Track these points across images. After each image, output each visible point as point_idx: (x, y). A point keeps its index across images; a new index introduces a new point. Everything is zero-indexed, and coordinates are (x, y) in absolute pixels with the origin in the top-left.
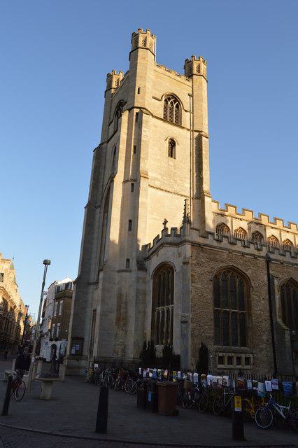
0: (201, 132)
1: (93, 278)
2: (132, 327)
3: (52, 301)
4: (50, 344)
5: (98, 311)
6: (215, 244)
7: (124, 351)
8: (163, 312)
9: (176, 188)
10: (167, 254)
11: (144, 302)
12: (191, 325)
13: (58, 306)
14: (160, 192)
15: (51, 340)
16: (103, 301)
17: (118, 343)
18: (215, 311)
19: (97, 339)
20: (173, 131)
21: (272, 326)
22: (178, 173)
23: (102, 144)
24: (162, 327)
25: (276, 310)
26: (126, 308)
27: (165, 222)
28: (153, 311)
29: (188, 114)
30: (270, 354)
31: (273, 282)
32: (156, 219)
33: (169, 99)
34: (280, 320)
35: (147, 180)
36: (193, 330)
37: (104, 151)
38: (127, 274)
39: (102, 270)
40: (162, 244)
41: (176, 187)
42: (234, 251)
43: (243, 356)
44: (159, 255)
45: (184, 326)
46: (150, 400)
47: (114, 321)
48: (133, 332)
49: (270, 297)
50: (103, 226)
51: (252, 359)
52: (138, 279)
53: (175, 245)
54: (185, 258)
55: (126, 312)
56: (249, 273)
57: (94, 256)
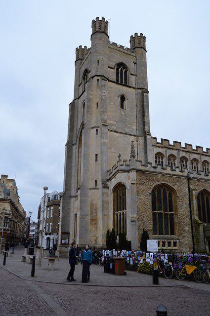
1: (73, 193)
2: (100, 224)
4: (45, 237)
5: (78, 215)
6: (152, 170)
7: (96, 240)
8: (120, 214)
9: (127, 130)
10: (121, 178)
11: (108, 209)
12: (138, 223)
13: (50, 211)
15: (46, 234)
16: (81, 208)
18: (154, 214)
20: (124, 90)
21: (191, 221)
22: (128, 119)
23: (74, 100)
24: (120, 222)
25: (194, 211)
26: (96, 212)
27: (120, 156)
28: (114, 214)
29: (133, 77)
30: (191, 239)
31: (192, 192)
32: (113, 152)
35: (106, 127)
36: (139, 225)
38: (96, 190)
39: (79, 189)
40: (118, 171)
42: (165, 174)
43: (172, 241)
45: (133, 223)
46: (111, 267)
47: (89, 221)
49: (190, 203)
50: (78, 157)
51: (178, 243)
52: (103, 194)
53: (126, 171)
56: (175, 187)
57: (73, 178)
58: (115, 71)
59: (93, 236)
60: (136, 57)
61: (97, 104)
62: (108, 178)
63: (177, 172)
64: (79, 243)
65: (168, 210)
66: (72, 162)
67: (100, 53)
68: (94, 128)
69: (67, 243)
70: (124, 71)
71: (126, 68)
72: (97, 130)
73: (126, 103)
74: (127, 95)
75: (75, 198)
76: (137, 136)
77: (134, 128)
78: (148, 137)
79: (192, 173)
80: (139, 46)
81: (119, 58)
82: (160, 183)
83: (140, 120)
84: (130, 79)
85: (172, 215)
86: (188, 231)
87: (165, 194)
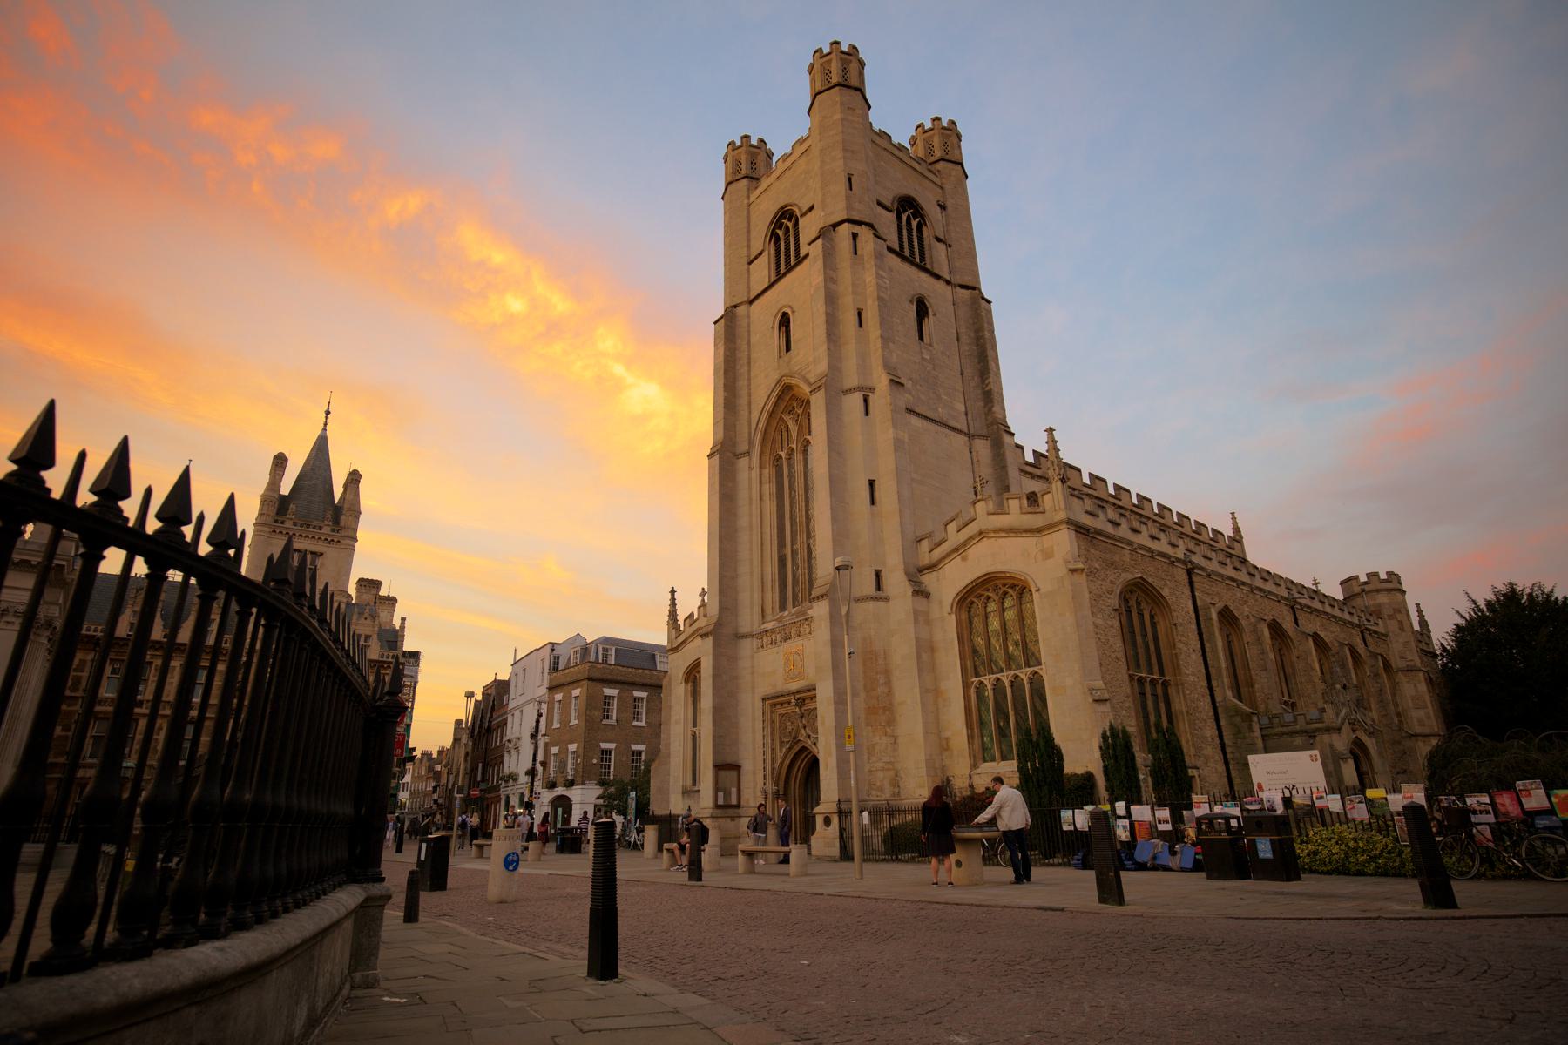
0: (974, 288)
2: (911, 722)
3: (543, 690)
5: (825, 692)
6: (1110, 529)
7: (895, 783)
9: (941, 413)
14: (915, 421)
17: (880, 765)
19: (833, 761)
20: (924, 283)
26: (888, 683)
28: (966, 686)
29: (942, 247)
30: (1221, 768)
33: (905, 211)
34: (1229, 693)
38: (881, 604)
40: (981, 534)
41: (940, 410)
50: (761, 499)
51: (1198, 779)
52: (916, 613)
56: (1165, 592)
57: (743, 569)
58: (892, 217)
59: (883, 769)
60: (942, 188)
61: (859, 314)
62: (926, 559)
63: (1162, 546)
65: (1156, 668)
67: (853, 152)
68: (855, 389)
69: (734, 802)
70: (914, 223)
71: (923, 218)
72: (866, 400)
73: (930, 323)
74: (932, 301)
76: (970, 436)
77: (956, 408)
78: (1006, 438)
79: (1195, 553)
80: (947, 157)
81: (901, 183)
82: (1130, 577)
83: (972, 384)
84: (934, 253)
85: (1165, 685)
87: (1141, 615)
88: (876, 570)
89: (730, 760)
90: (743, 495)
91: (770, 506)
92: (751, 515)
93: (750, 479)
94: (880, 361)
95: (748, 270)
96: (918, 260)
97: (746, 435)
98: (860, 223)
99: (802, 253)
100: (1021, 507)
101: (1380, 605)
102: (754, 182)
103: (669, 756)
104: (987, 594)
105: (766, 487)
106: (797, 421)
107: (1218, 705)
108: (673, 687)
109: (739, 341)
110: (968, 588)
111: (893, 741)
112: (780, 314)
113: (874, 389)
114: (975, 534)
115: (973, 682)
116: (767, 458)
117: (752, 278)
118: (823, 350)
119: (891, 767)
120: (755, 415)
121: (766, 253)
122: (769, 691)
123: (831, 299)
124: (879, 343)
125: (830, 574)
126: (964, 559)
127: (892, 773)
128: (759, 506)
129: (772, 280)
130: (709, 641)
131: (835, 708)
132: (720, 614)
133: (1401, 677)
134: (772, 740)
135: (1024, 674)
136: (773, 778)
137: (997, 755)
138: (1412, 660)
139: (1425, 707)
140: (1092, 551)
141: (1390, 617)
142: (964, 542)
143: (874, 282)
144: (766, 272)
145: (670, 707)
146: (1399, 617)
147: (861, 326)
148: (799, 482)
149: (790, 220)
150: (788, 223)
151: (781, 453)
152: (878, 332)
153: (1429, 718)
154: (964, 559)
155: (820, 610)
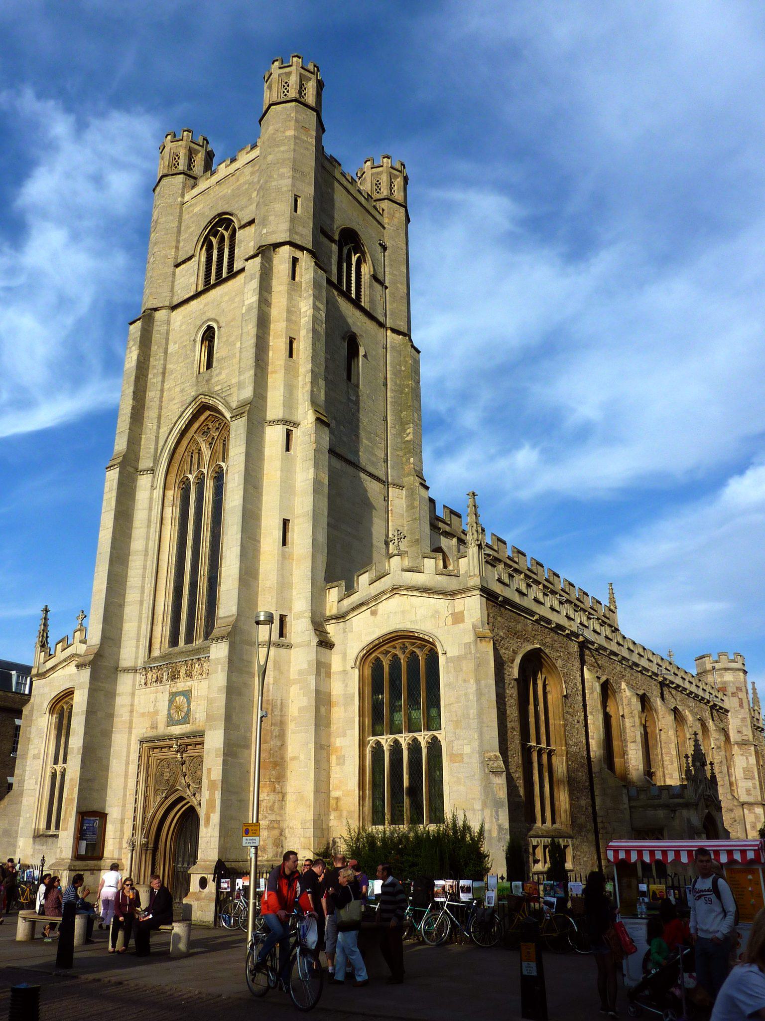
6: (517, 598)
19: (215, 818)
21: (591, 779)
26: (282, 736)
28: (362, 744)
33: (346, 244)
37: (163, 329)
38: (283, 651)
44: (380, 612)
48: (311, 796)
50: (161, 523)
53: (438, 593)
54: (474, 627)
55: (283, 746)
64: (222, 849)
65: (543, 738)
66: (130, 537)
71: (363, 253)
72: (289, 434)
75: (140, 678)
82: (529, 647)
85: (550, 754)
86: (587, 809)
88: (280, 615)
89: (95, 807)
90: (140, 515)
91: (170, 533)
92: (148, 539)
93: (151, 499)
94: (308, 396)
95: (174, 274)
96: (353, 296)
97: (152, 451)
98: (301, 248)
99: (237, 266)
100: (436, 568)
101: (725, 683)
102: (192, 181)
103: (21, 794)
104: (393, 651)
105: (168, 511)
106: (211, 444)
107: (593, 775)
108: (34, 718)
109: (154, 348)
110: (374, 644)
111: (281, 799)
112: (204, 327)
113: (298, 425)
114: (387, 590)
115: (369, 742)
116: (172, 478)
117: (176, 283)
118: (249, 375)
119: (276, 825)
120: (164, 430)
121: (195, 259)
122: (151, 733)
123: (263, 322)
124: (308, 379)
125: (233, 615)
126: (374, 613)
127: (276, 832)
128: (158, 530)
129: (199, 290)
130: (86, 673)
131: (223, 760)
132: (101, 644)
133: (736, 749)
134: (146, 787)
135: (423, 738)
136: (143, 829)
137: (387, 817)
138: (746, 735)
139: (753, 778)
140: (499, 619)
141: (734, 695)
142: (375, 596)
143: (310, 312)
144: (194, 279)
145: (29, 739)
146: (742, 695)
147: (291, 355)
148: (208, 508)
149: (226, 229)
150: (224, 232)
151: (190, 476)
152: (309, 366)
153: (755, 788)
154: (374, 613)
155: (219, 651)
